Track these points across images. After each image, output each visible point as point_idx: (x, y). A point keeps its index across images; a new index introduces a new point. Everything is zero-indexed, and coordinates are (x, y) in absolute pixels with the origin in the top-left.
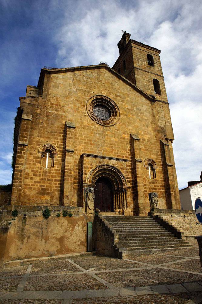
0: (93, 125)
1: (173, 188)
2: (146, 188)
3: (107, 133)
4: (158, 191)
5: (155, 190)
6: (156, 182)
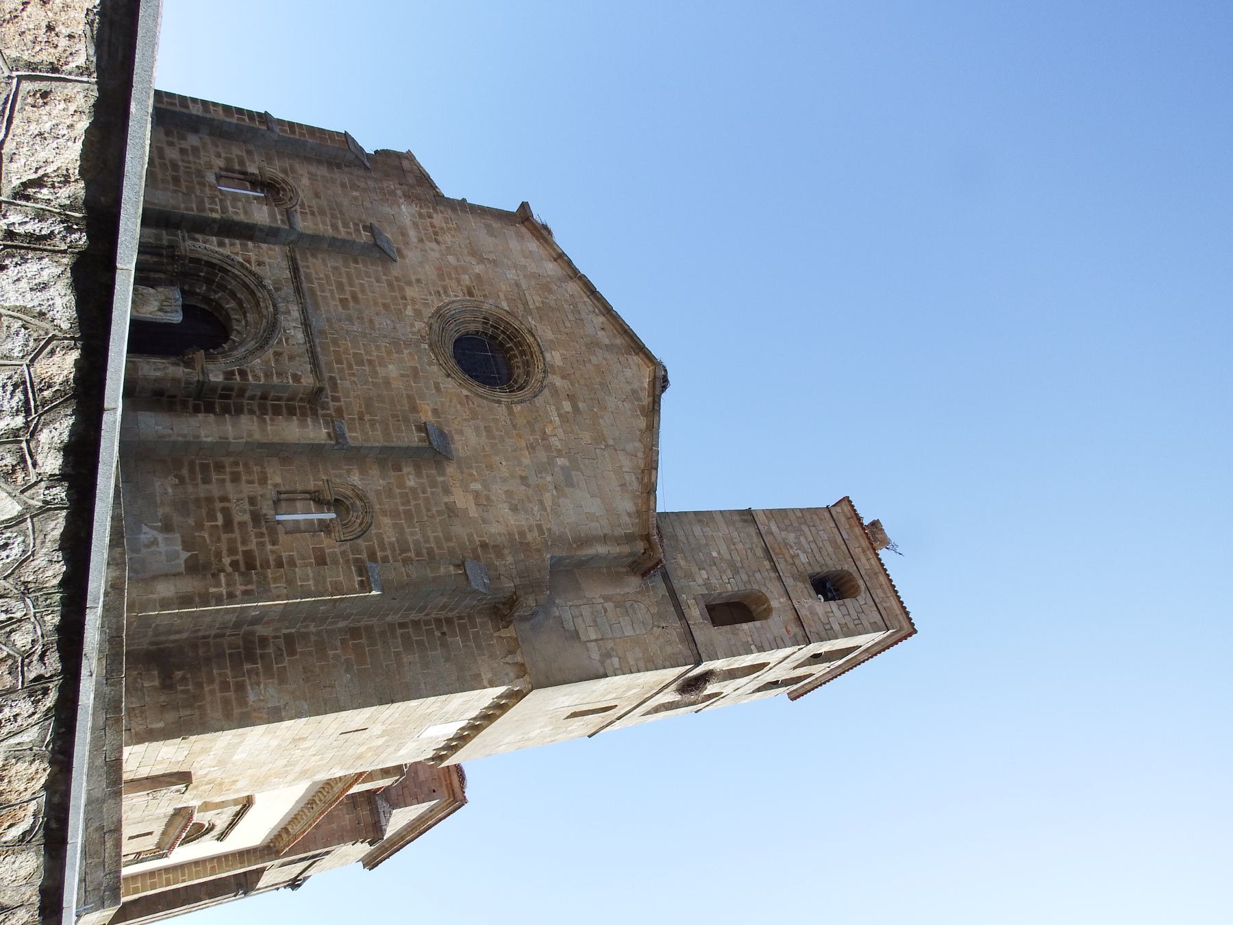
0: (418, 313)
1: (249, 587)
2: (223, 481)
3: (410, 353)
4: (219, 540)
5: (220, 522)
6: (264, 530)
